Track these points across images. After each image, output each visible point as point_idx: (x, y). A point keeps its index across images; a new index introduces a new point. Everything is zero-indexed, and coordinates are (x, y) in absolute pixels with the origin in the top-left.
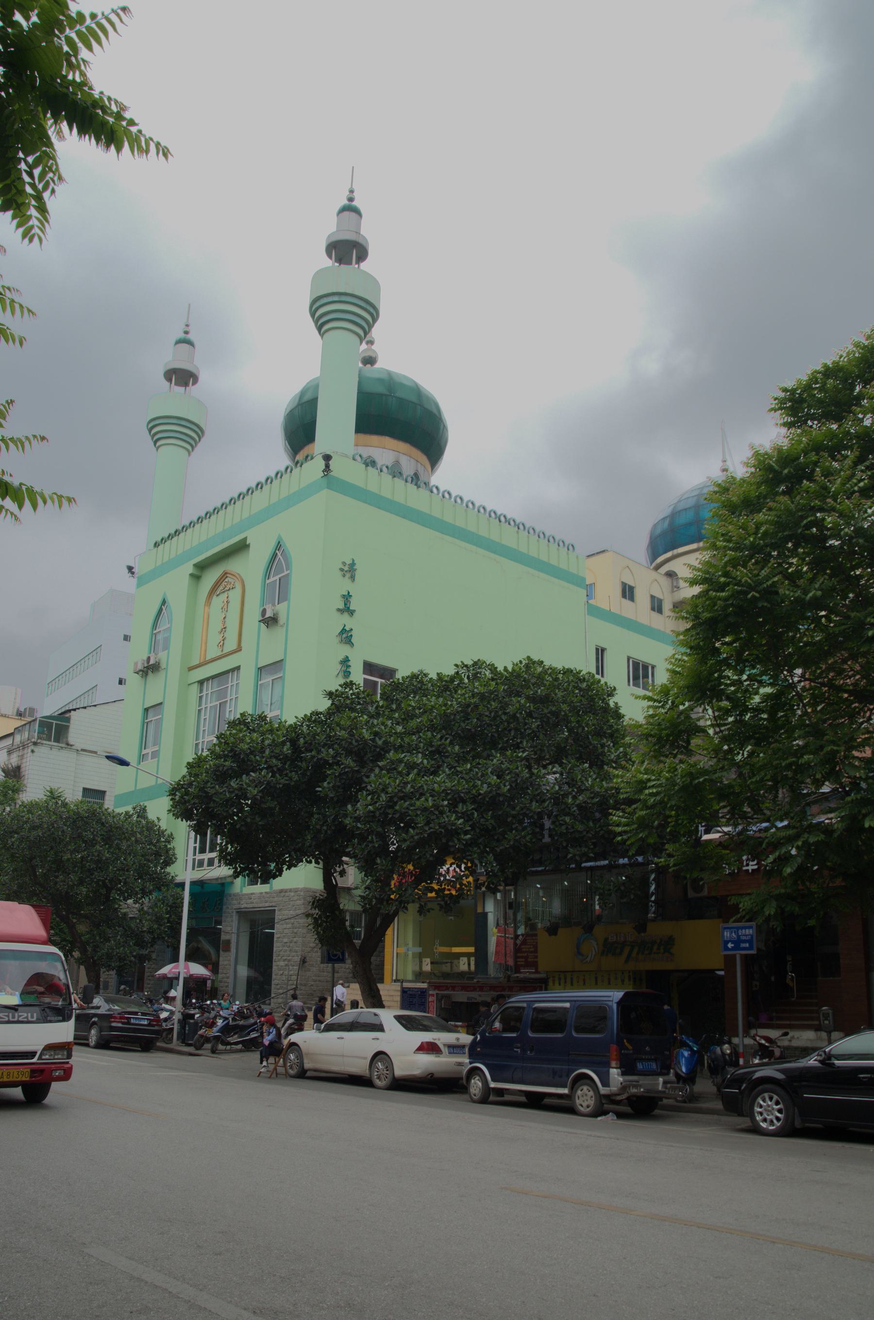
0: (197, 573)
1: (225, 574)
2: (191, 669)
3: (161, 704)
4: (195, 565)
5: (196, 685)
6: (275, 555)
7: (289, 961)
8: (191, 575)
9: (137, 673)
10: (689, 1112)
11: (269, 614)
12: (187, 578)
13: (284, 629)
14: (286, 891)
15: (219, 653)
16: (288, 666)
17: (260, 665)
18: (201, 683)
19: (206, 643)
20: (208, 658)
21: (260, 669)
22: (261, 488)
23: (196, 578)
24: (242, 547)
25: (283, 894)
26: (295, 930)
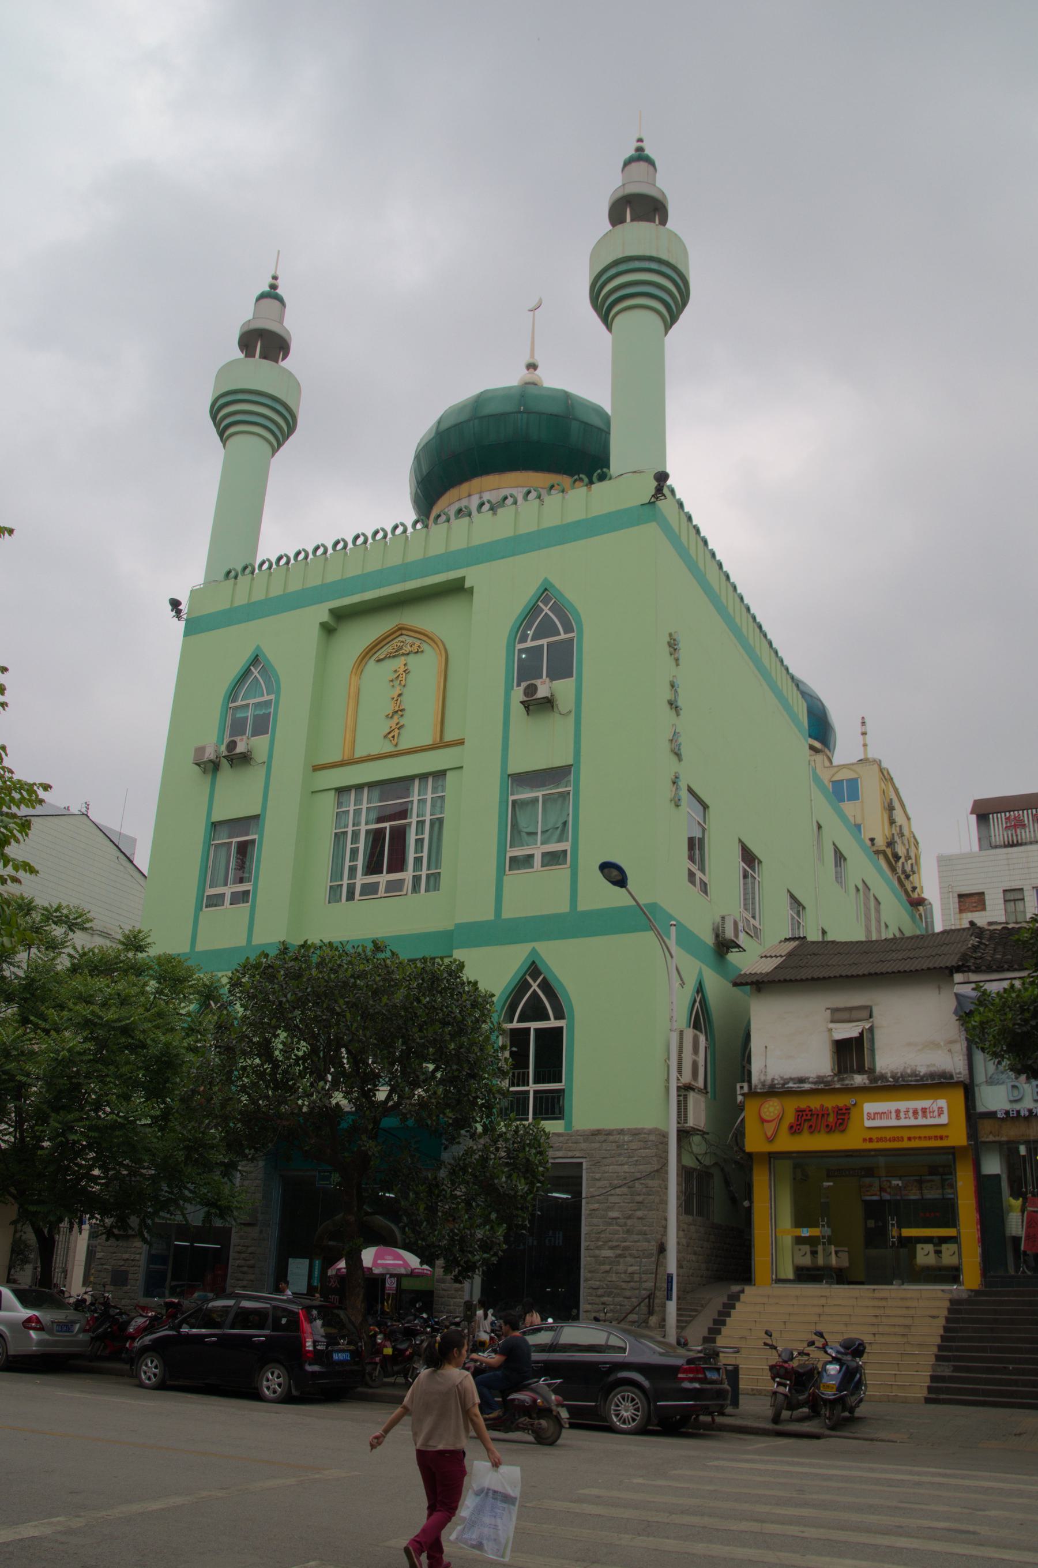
0: (332, 623)
1: (400, 630)
2: (316, 768)
3: (257, 817)
4: (333, 612)
5: (332, 795)
6: (247, 672)
7: (626, 1248)
8: (324, 626)
9: (198, 764)
10: (725, 1430)
11: (240, 748)
12: (315, 631)
13: (262, 772)
14: (609, 1133)
15: (388, 748)
16: (586, 775)
17: (215, 818)
18: (342, 791)
19: (354, 731)
20: (358, 754)
21: (215, 825)
22: (236, 577)
23: (328, 630)
24: (457, 589)
25: (601, 1138)
26: (639, 1198)
